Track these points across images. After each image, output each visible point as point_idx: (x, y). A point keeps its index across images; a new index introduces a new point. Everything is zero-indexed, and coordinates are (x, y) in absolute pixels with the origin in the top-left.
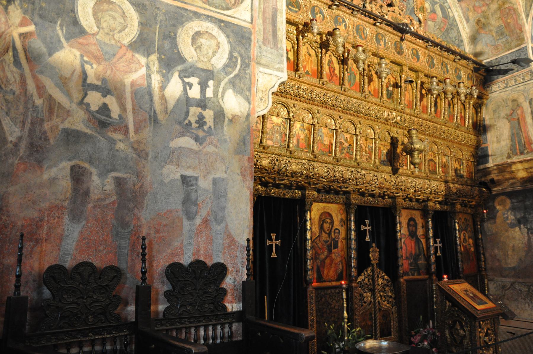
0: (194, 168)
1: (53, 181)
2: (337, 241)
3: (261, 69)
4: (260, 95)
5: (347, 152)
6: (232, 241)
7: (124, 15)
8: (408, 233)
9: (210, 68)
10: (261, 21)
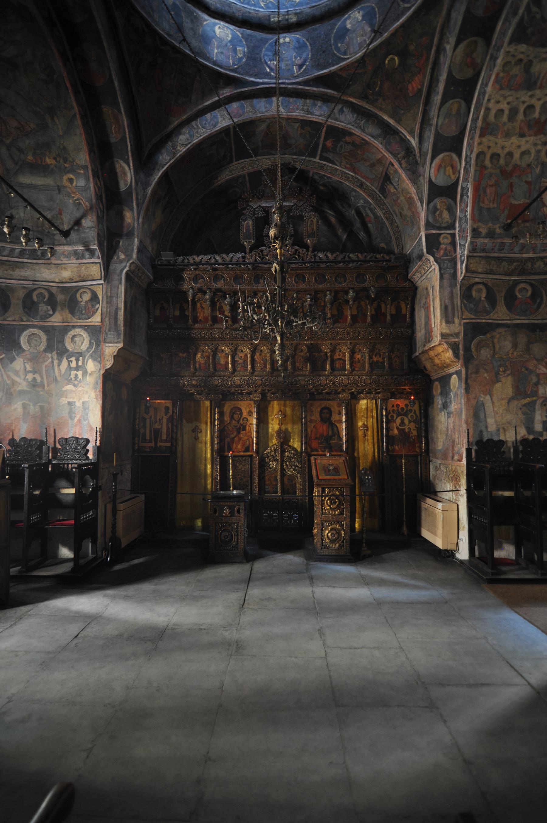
0: (74, 398)
1: (16, 409)
2: (245, 427)
3: (107, 345)
4: (107, 358)
5: (242, 366)
6: (92, 428)
7: (40, 338)
8: (320, 419)
9: (80, 351)
10: (108, 318)
